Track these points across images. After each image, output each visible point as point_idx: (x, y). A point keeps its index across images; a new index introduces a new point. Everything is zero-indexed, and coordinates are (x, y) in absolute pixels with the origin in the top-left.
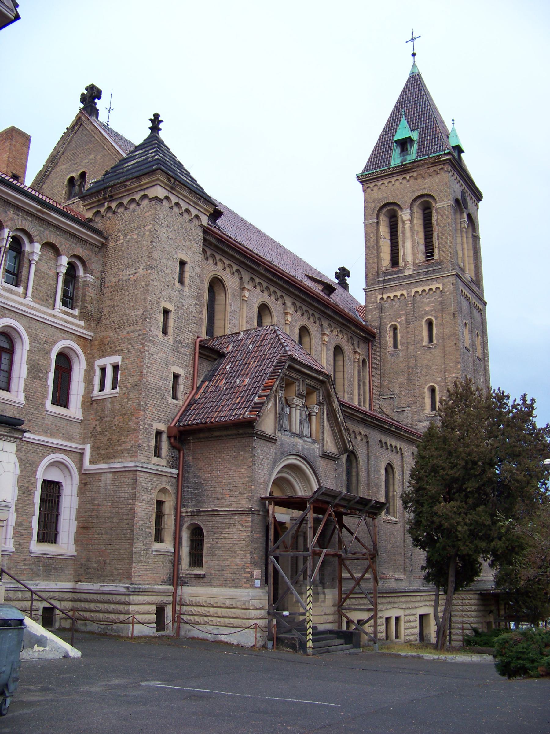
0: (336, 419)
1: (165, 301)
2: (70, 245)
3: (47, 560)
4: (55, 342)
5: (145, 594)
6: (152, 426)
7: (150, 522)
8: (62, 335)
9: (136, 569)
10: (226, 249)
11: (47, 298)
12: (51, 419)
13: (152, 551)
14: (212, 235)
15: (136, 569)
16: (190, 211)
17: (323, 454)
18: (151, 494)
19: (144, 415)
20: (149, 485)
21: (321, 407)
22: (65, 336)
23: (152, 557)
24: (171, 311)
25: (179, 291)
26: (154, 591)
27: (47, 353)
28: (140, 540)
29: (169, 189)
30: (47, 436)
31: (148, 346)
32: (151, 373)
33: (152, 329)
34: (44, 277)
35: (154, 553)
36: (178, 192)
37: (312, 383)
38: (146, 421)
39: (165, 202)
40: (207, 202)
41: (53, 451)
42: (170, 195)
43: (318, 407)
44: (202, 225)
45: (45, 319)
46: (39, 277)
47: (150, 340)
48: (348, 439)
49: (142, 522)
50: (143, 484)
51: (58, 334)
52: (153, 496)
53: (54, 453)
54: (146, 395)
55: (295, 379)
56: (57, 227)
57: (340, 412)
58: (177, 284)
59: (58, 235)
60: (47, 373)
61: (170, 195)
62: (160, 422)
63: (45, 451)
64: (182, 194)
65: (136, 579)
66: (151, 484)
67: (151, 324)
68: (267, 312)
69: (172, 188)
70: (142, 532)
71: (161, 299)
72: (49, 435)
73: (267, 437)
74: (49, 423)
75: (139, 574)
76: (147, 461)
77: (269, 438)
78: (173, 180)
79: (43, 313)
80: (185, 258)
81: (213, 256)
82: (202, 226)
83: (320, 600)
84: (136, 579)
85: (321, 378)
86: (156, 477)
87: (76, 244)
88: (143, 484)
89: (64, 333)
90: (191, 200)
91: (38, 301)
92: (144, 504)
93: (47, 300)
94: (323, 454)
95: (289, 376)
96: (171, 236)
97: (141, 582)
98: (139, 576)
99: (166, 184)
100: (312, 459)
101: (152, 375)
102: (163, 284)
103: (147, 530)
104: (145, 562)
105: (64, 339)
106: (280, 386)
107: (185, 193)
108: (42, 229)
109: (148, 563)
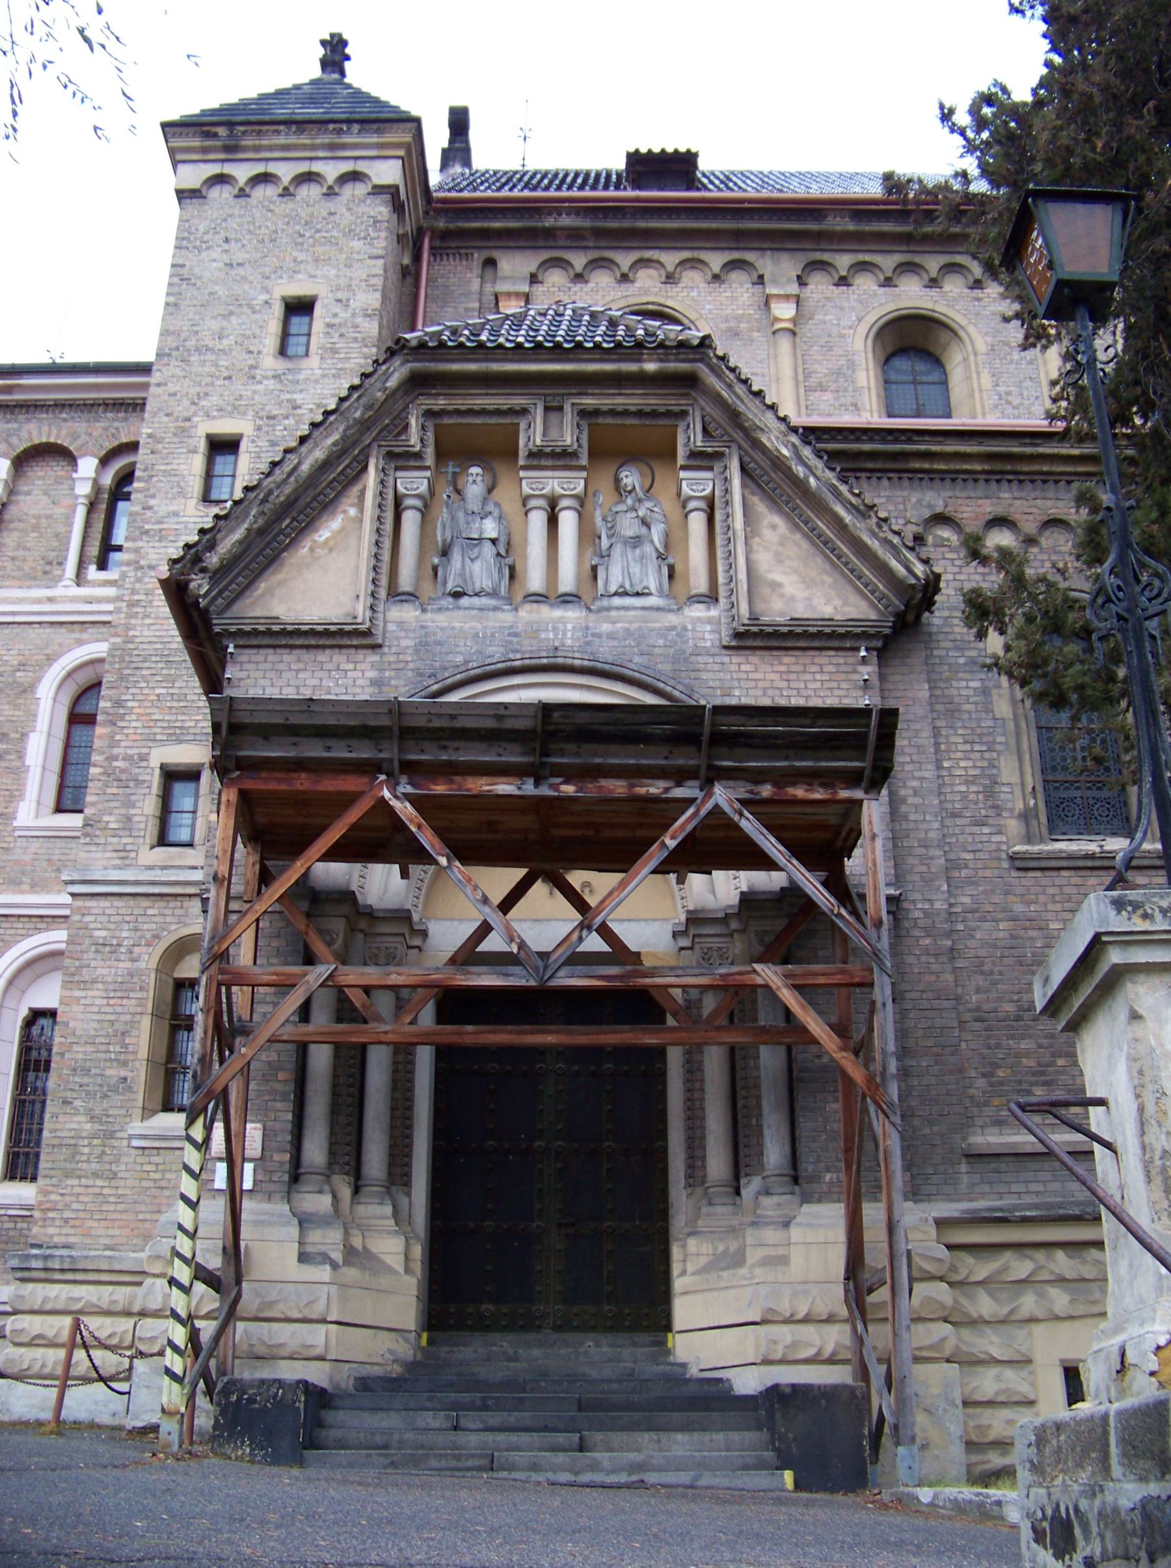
0: (799, 485)
1: (214, 418)
2: (106, 429)
3: (11, 1225)
4: (51, 659)
5: (79, 1276)
6: (144, 758)
7: (126, 1046)
8: (76, 635)
9: (53, 1197)
10: (642, 224)
11: (48, 568)
12: (35, 846)
13: (131, 1137)
14: (559, 212)
15: (53, 1197)
16: (318, 174)
17: (738, 635)
18: (133, 960)
19: (111, 737)
20: (125, 934)
21: (718, 467)
22: (85, 636)
23: (131, 1157)
24: (241, 436)
25: (274, 377)
26: (117, 1267)
27: (24, 691)
28: (77, 1103)
29: (222, 156)
30: (23, 892)
31: (137, 551)
32: (146, 616)
33: (152, 502)
34: (36, 528)
35: (135, 1143)
36: (257, 149)
37: (619, 400)
38: (116, 751)
39: (215, 193)
40: (375, 126)
41: (39, 926)
42: (228, 169)
43: (708, 475)
44: (375, 187)
45: (14, 613)
46: (22, 530)
47: (147, 532)
48: (886, 542)
49: (89, 1048)
50: (97, 933)
51: (62, 634)
52: (142, 965)
53: (39, 930)
54: (122, 678)
55: (498, 412)
56: (61, 405)
57: (807, 452)
58: (270, 362)
59: (65, 420)
60: (24, 736)
61: (228, 169)
62: (181, 742)
63: (12, 932)
64: (271, 148)
65: (51, 1230)
66: (136, 930)
67: (152, 491)
68: (944, 336)
69: (228, 149)
70: (86, 1080)
71: (196, 419)
72: (25, 887)
73: (297, 633)
74: (27, 858)
75: (67, 1214)
76: (118, 862)
77: (313, 633)
78: (222, 131)
79: (13, 603)
80: (298, 288)
81: (597, 264)
82: (378, 190)
83: (753, 1256)
84: (51, 1230)
85: (651, 367)
86: (161, 904)
87: (126, 419)
88: (97, 933)
89: (81, 631)
90: (313, 147)
91: (18, 583)
92: (103, 994)
93: (45, 573)
94: (738, 635)
95: (457, 412)
96: (240, 256)
97: (71, 1240)
98: (66, 1221)
99: (205, 150)
100: (665, 667)
101: (148, 621)
102: (208, 380)
103: (109, 1072)
104: (95, 1175)
105: (80, 643)
106: (390, 456)
107: (281, 140)
108: (16, 425)
109: (114, 1176)
